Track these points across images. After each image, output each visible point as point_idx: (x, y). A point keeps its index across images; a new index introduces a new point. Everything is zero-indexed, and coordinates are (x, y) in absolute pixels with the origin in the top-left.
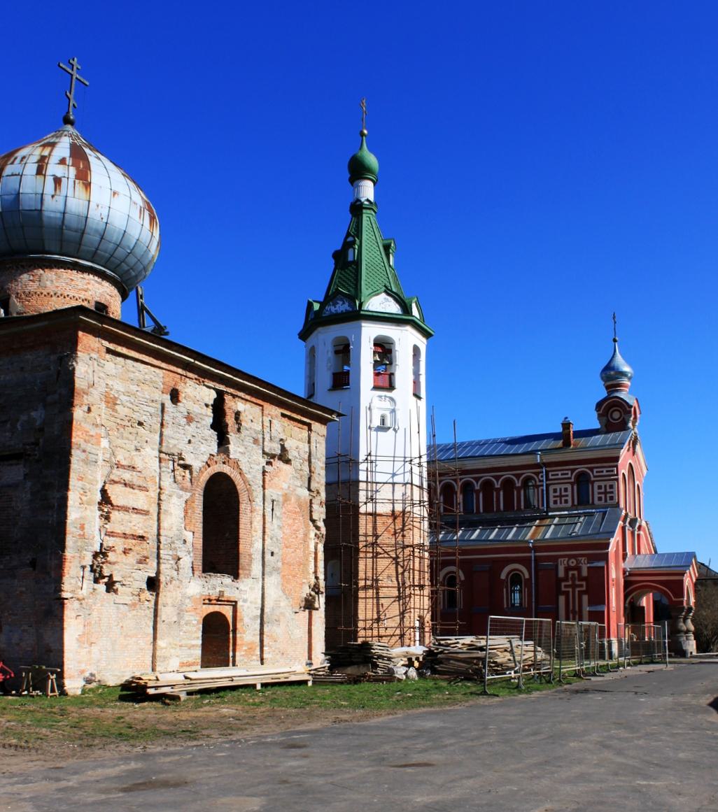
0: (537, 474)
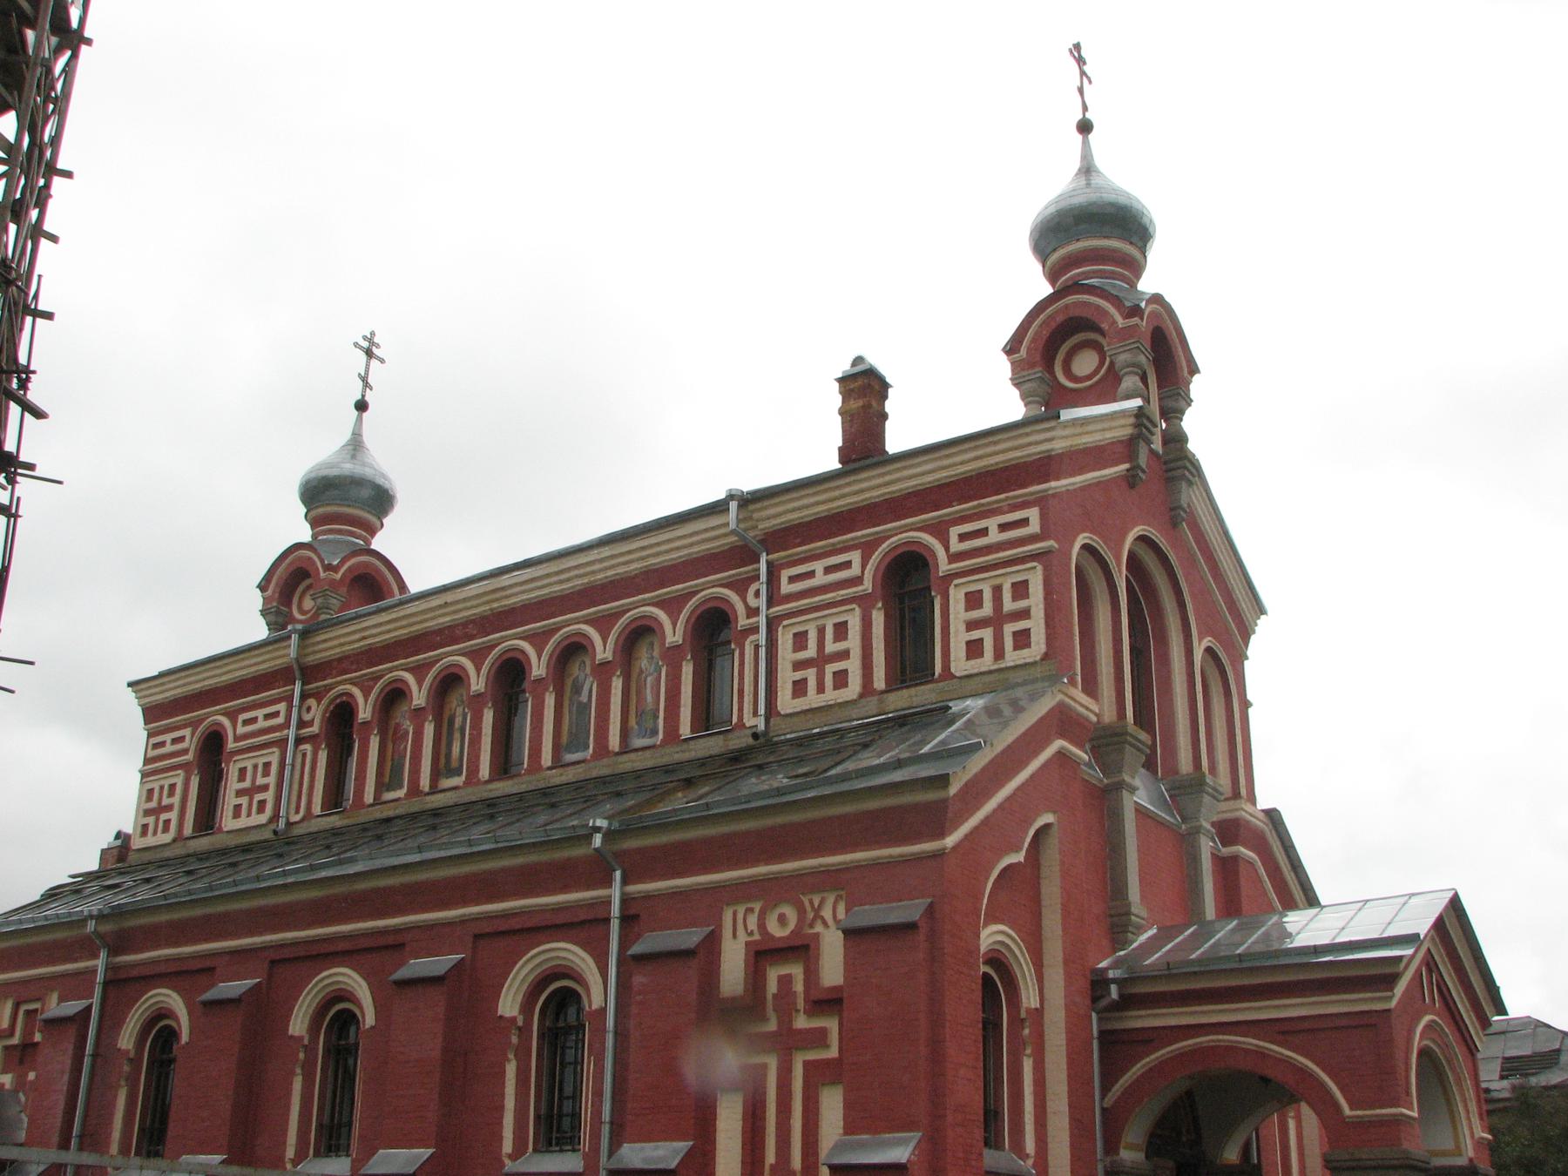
0: (740, 586)
